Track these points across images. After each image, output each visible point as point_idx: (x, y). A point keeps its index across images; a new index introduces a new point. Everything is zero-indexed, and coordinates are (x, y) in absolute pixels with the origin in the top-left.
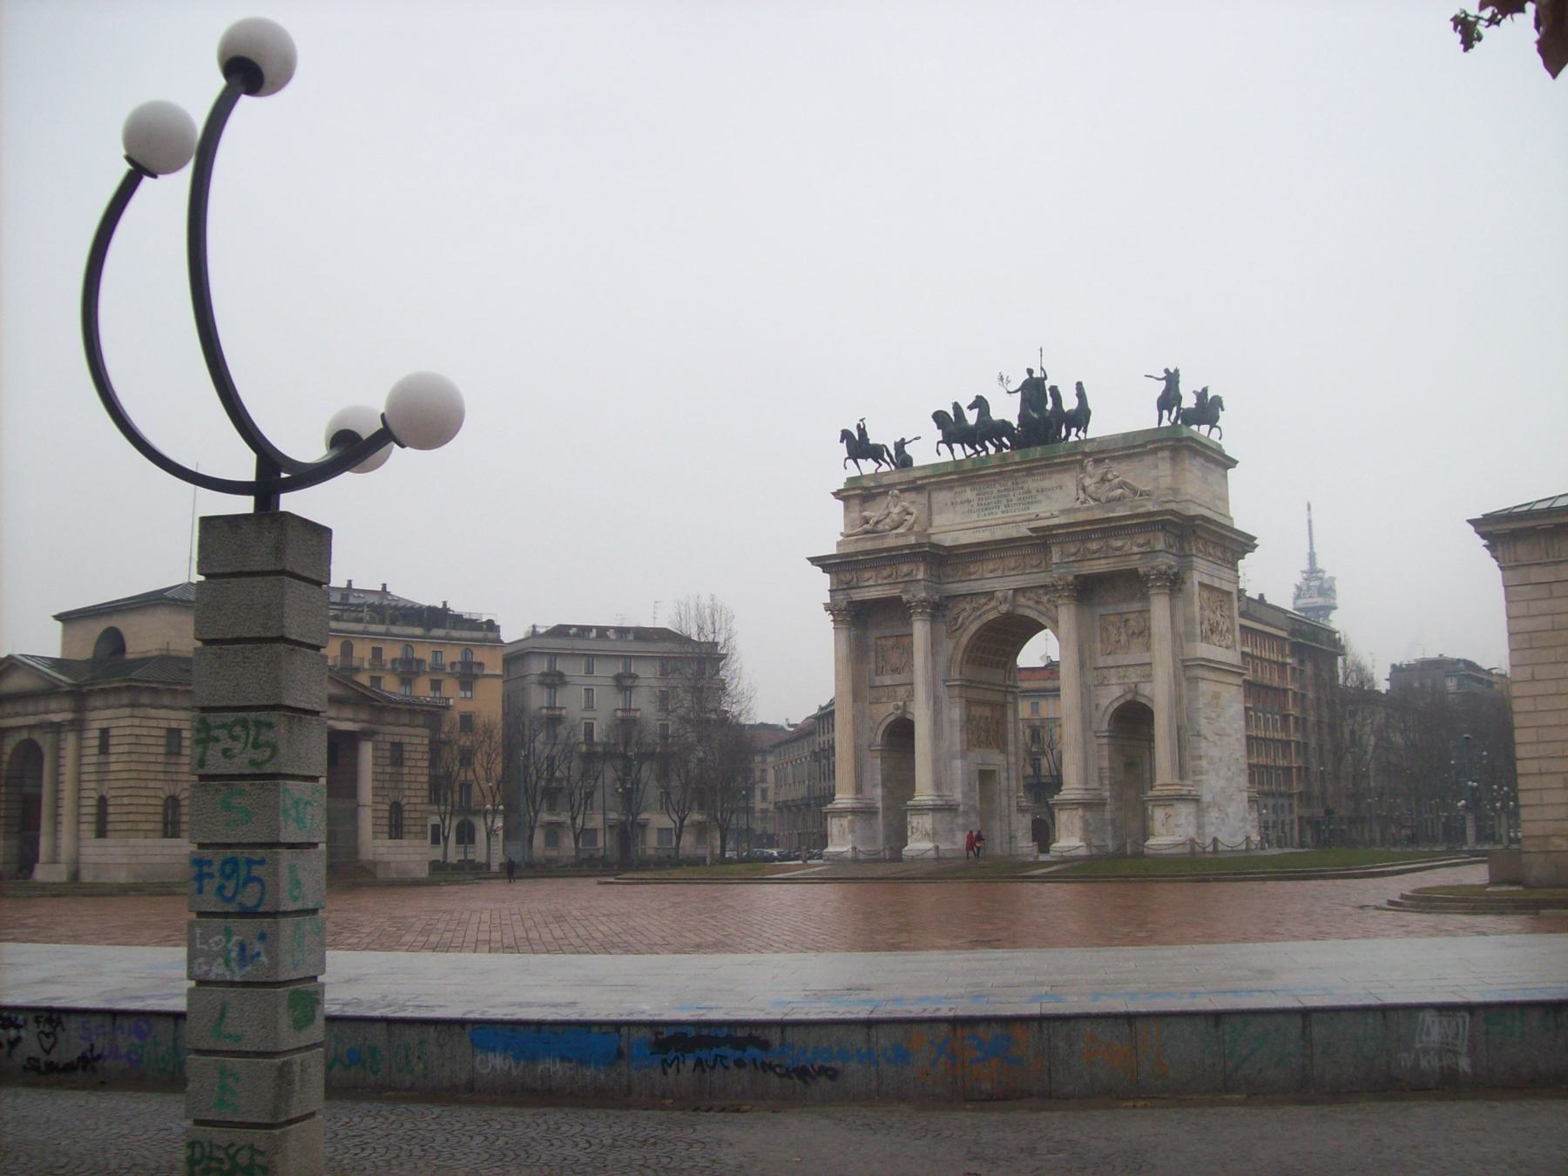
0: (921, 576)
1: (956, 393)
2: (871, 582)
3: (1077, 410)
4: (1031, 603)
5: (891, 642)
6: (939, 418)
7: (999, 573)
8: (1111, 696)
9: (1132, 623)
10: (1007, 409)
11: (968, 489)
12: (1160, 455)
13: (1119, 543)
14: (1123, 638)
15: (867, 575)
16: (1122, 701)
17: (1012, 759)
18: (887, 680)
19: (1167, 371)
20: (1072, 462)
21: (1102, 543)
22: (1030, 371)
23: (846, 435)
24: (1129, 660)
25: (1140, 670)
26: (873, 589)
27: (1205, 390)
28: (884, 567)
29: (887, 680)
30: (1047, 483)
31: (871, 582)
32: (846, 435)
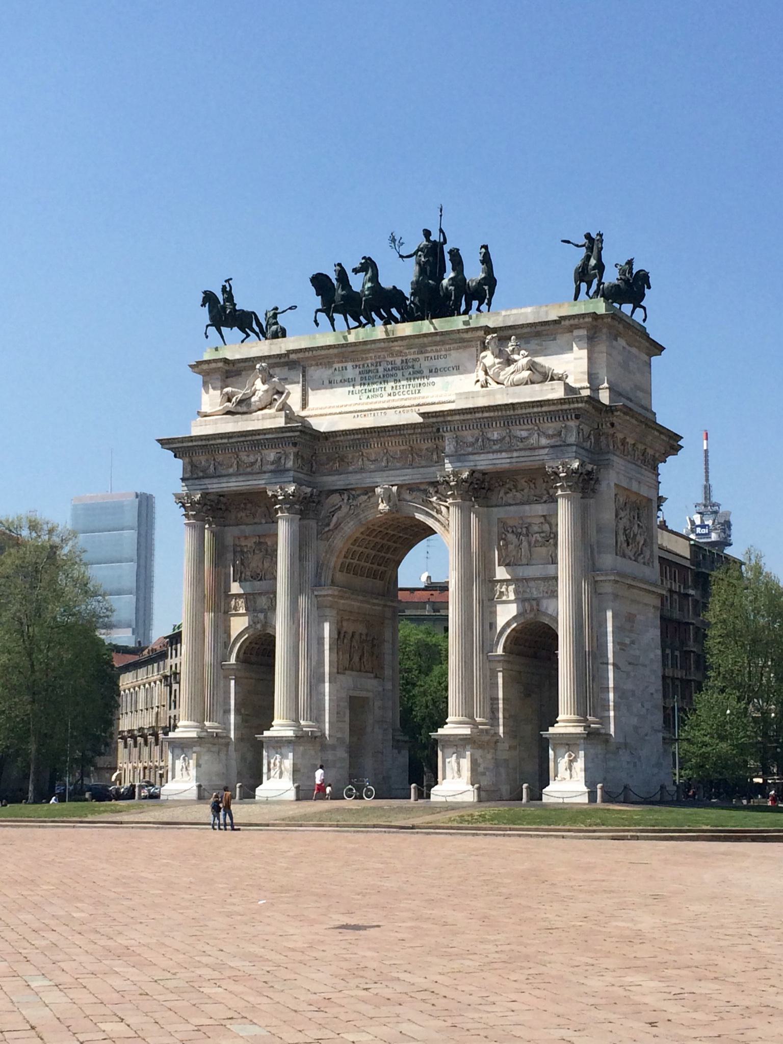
1: (338, 253)
2: (231, 471)
6: (320, 282)
10: (400, 276)
11: (349, 365)
12: (576, 333)
13: (524, 434)
14: (525, 544)
17: (389, 686)
19: (588, 236)
22: (427, 233)
23: (209, 298)
25: (542, 586)
27: (630, 263)
31: (231, 471)
32: (209, 298)
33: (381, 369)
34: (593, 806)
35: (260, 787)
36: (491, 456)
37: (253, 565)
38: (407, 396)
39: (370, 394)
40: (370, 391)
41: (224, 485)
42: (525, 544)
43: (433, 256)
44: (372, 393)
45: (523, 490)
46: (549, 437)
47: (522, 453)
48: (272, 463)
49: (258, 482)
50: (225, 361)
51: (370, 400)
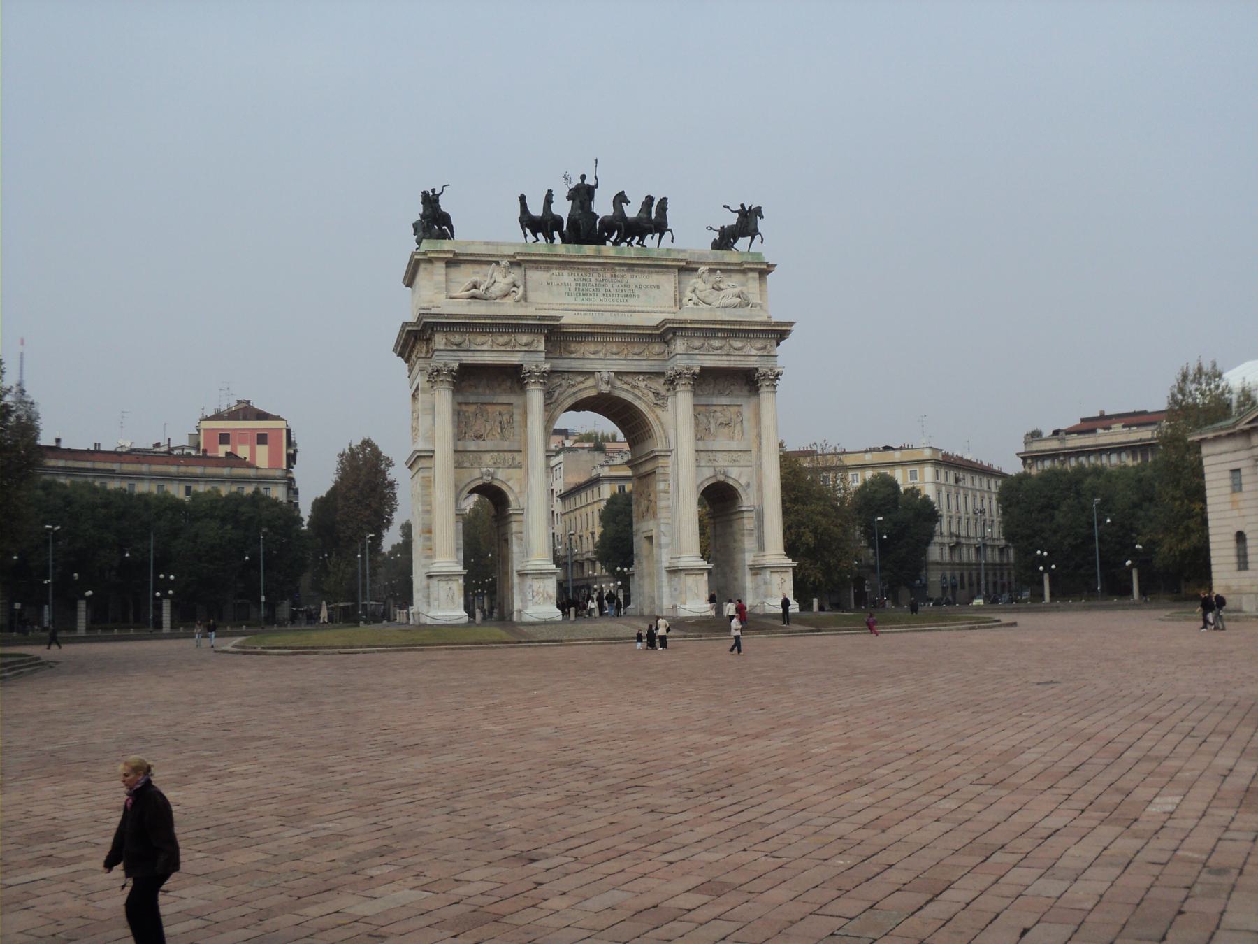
0: (542, 347)
3: (614, 217)
4: (625, 387)
5: (472, 409)
7: (601, 355)
8: (707, 476)
9: (719, 414)
11: (566, 273)
12: (751, 275)
15: (480, 339)
16: (712, 481)
18: (472, 446)
19: (742, 206)
20: (672, 267)
21: (723, 342)
22: (583, 177)
23: (425, 194)
24: (716, 446)
25: (727, 456)
26: (486, 352)
29: (472, 446)
31: (485, 347)
33: (593, 279)
34: (806, 614)
37: (476, 428)
42: (712, 427)
43: (583, 194)
46: (758, 349)
48: (526, 345)
49: (515, 359)
50: (455, 254)
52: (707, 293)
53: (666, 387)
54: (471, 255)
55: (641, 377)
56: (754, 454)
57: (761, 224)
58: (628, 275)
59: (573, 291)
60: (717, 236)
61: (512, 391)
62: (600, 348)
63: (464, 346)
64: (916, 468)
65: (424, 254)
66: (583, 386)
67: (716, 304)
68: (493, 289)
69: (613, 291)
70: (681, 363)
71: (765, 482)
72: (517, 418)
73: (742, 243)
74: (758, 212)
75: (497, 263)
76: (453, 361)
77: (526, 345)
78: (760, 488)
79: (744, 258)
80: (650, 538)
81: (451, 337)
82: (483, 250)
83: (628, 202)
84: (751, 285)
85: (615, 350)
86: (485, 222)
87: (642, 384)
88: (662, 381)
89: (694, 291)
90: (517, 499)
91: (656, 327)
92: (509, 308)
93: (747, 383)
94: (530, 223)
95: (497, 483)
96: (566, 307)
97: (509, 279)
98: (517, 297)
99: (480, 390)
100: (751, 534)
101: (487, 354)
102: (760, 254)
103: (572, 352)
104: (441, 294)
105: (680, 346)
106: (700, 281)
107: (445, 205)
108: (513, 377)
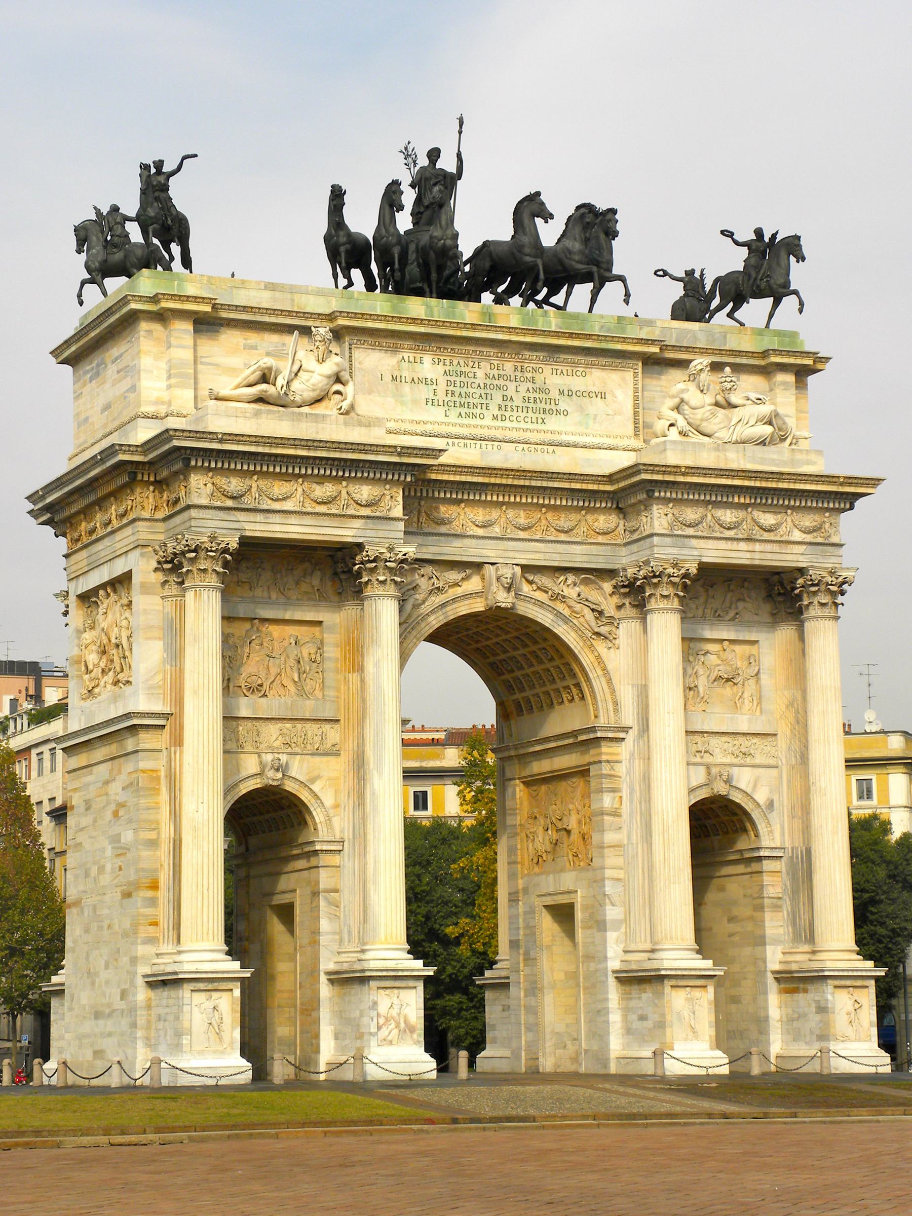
0: (398, 511)
4: (539, 595)
7: (497, 530)
9: (712, 659)
11: (427, 358)
12: (781, 377)
15: (279, 488)
19: (759, 233)
21: (741, 514)
22: (434, 154)
28: (321, 480)
30: (577, 383)
31: (288, 506)
33: (480, 374)
35: (483, 1054)
36: (723, 545)
38: (522, 425)
39: (463, 411)
40: (462, 405)
41: (278, 528)
44: (467, 411)
45: (696, 598)
47: (769, 547)
49: (347, 533)
51: (460, 421)
52: (700, 414)
53: (615, 600)
54: (245, 309)
55: (571, 578)
56: (782, 742)
57: (799, 274)
58: (547, 369)
59: (441, 395)
60: (677, 291)
61: (319, 598)
62: (495, 514)
63: (248, 501)
64: (871, 775)
65: (155, 299)
66: (459, 591)
67: (724, 435)
68: (296, 385)
69: (518, 401)
70: (664, 553)
71: (816, 802)
72: (331, 652)
73: (755, 310)
74: (793, 246)
75: (306, 331)
76: (228, 530)
77: (368, 505)
78: (803, 810)
79: (767, 343)
80: (563, 914)
81: (221, 481)
82: (263, 299)
83: (547, 216)
84: (783, 397)
85: (522, 521)
86: (259, 240)
87: (571, 593)
88: (608, 586)
89: (677, 408)
90: (329, 820)
91: (610, 478)
92: (329, 427)
93: (769, 597)
94: (345, 251)
95: (290, 786)
96: (429, 428)
97: (331, 366)
98: (345, 405)
99: (259, 592)
100: (777, 908)
101: (293, 519)
102: (793, 335)
103: (442, 522)
104: (170, 384)
105: (658, 518)
106: (692, 387)
107: (182, 195)
108: (337, 569)
